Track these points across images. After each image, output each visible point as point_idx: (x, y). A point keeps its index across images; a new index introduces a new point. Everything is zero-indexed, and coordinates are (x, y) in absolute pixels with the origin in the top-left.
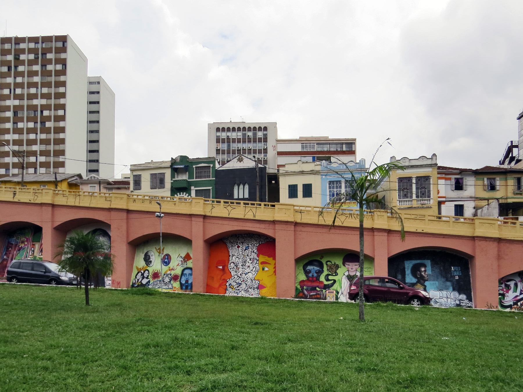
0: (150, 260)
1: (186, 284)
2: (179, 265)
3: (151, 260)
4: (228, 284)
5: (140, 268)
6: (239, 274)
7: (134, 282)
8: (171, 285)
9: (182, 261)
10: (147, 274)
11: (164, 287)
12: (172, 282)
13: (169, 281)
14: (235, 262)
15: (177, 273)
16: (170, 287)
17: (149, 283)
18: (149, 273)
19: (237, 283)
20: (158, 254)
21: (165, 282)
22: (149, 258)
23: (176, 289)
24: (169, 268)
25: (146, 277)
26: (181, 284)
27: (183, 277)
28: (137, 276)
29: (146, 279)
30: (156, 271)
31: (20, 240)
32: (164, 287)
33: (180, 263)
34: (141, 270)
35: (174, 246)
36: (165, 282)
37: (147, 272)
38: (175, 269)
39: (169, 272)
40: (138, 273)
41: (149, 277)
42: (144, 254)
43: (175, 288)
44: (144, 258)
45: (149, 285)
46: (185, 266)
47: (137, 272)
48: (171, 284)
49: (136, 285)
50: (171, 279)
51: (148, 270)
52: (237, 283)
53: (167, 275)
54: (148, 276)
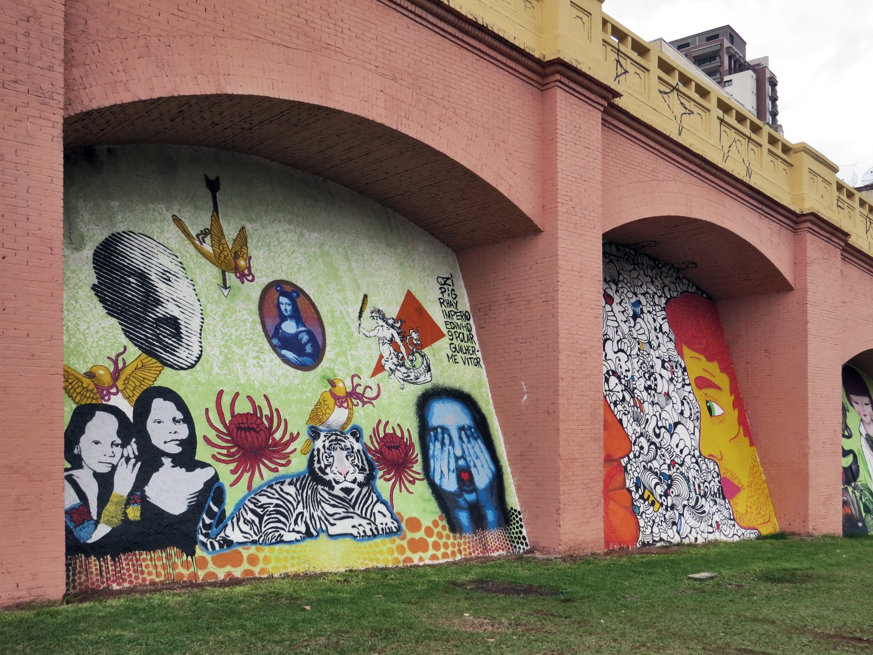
0: (160, 311)
1: (471, 497)
2: (388, 365)
3: (172, 310)
4: (630, 484)
5: (90, 375)
6: (650, 428)
8: (380, 507)
9: (392, 341)
11: (343, 526)
12: (382, 486)
13: (361, 478)
14: (619, 371)
15: (393, 423)
16: (384, 521)
17: (219, 497)
18: (188, 419)
19: (656, 474)
20: (212, 273)
21: (337, 491)
22: (151, 298)
23: (421, 534)
24: (332, 383)
25: (177, 450)
26: (437, 492)
27: (435, 448)
29: (181, 472)
30: (244, 407)
32: (343, 526)
33: (387, 350)
34: (103, 391)
35: (314, 237)
36: (337, 491)
37: (161, 408)
38: (369, 394)
39: (338, 416)
41: (203, 453)
43: (415, 524)
45: (221, 519)
46: (426, 382)
48: (380, 500)
49: (103, 530)
50: (372, 468)
51: (168, 394)
52: (656, 474)
53: (337, 437)
54: (189, 444)
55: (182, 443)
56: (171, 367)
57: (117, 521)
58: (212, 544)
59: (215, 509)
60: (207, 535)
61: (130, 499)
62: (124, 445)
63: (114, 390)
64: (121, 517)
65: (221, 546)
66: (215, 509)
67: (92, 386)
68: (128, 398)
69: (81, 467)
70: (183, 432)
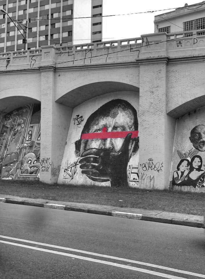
5: (185, 154)
7: (176, 176)
10: (197, 162)
18: (201, 161)
25: (197, 167)
28: (181, 166)
29: (197, 172)
31: (17, 122)
37: (197, 160)
40: (182, 161)
42: (190, 131)
44: (190, 138)
47: (179, 160)
49: (180, 182)
54: (200, 167)
55: (199, 166)
56: (201, 151)
57: (183, 180)
58: (200, 186)
59: (202, 179)
60: (199, 184)
61: (186, 177)
62: (187, 167)
63: (188, 156)
64: (184, 179)
65: (201, 187)
66: (202, 179)
67: (185, 156)
68: (190, 158)
69: (179, 170)
70: (200, 164)
